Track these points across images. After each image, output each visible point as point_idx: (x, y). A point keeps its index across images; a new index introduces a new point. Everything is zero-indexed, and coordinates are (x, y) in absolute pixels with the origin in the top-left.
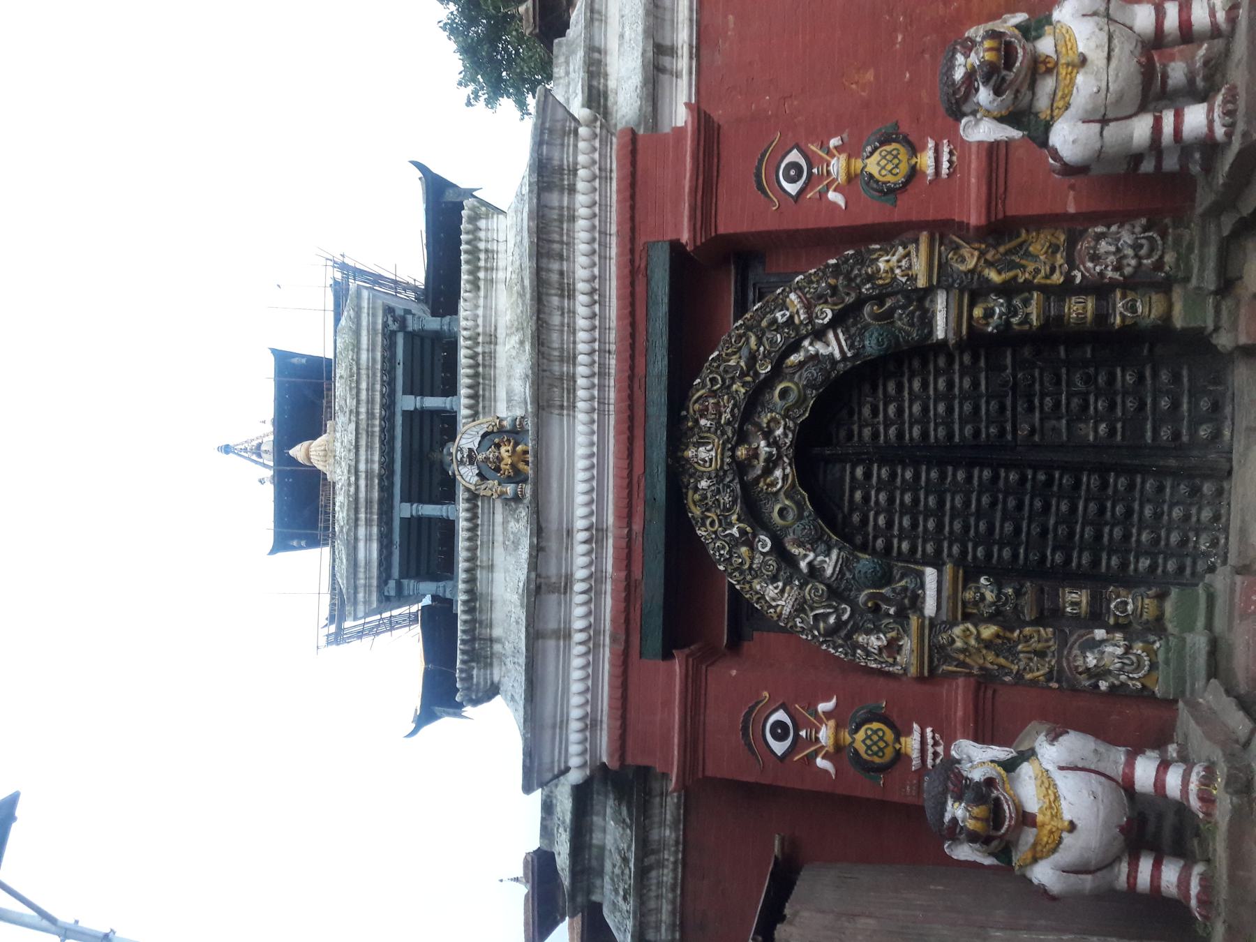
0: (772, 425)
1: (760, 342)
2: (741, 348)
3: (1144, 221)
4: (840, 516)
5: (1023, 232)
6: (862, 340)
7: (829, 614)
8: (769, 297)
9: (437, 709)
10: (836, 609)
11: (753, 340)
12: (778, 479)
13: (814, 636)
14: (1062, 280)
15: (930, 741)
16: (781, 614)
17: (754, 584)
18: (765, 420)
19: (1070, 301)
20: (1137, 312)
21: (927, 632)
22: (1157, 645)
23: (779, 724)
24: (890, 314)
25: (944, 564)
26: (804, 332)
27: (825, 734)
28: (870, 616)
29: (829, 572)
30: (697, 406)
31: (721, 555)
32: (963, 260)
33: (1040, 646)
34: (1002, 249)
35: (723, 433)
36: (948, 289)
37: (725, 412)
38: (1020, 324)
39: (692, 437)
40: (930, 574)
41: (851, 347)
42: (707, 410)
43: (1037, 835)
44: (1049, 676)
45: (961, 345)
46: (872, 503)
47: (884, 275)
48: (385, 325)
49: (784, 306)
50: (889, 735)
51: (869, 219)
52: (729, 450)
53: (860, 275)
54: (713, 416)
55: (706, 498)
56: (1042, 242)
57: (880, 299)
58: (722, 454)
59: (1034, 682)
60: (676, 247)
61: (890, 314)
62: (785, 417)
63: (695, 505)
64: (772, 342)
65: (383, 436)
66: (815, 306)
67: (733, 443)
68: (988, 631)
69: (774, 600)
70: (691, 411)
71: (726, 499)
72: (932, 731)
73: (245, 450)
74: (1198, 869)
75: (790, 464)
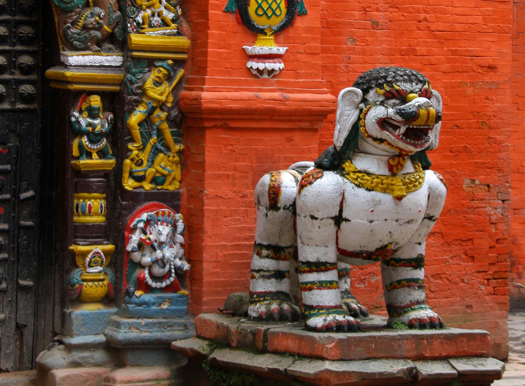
3: (186, 266)
14: (127, 188)
19: (104, 198)
20: (90, 266)
36: (124, 68)
38: (81, 147)
56: (169, 168)
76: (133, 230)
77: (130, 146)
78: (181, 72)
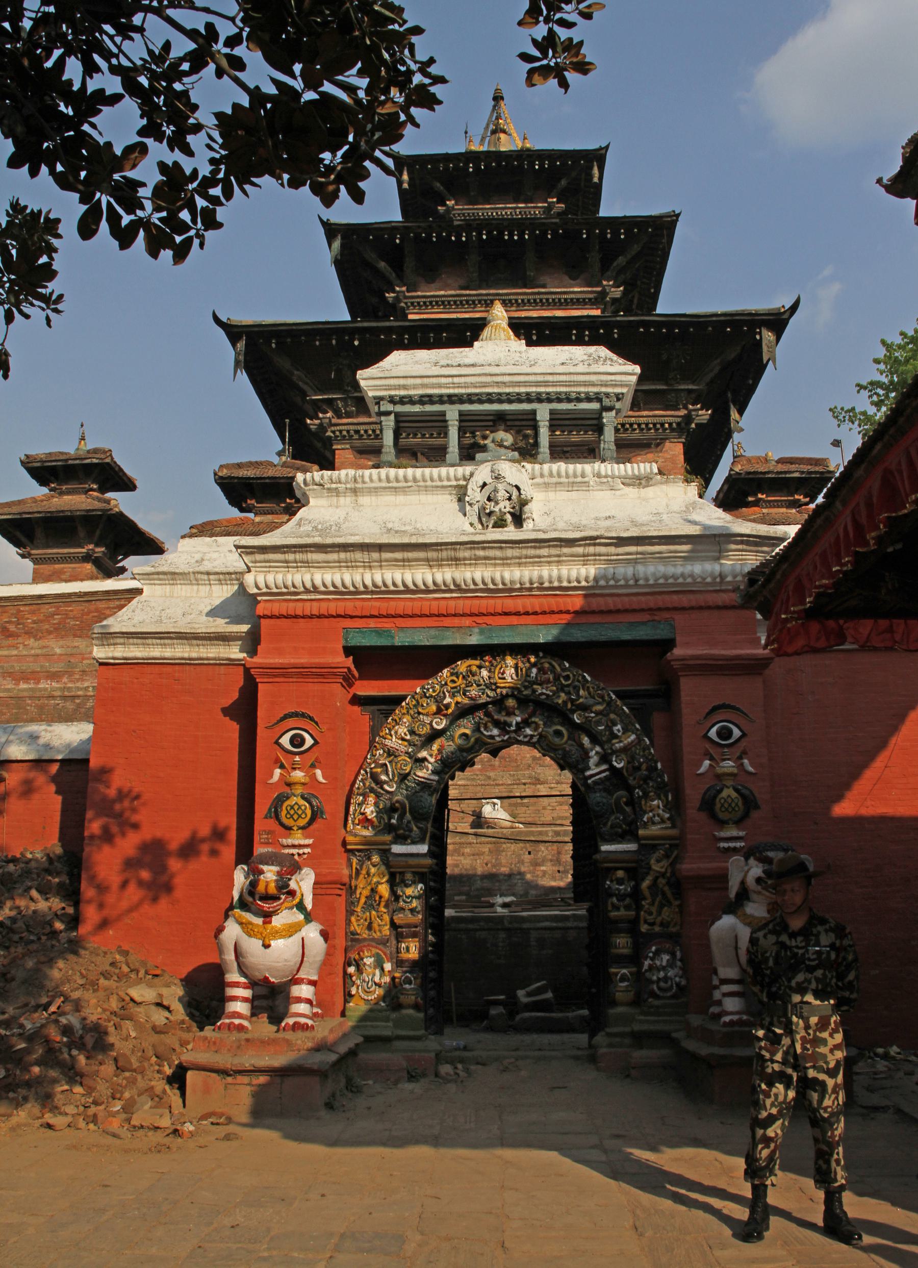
0: (533, 725)
1: (598, 713)
3: (683, 982)
5: (677, 903)
6: (600, 790)
7: (387, 775)
8: (634, 720)
9: (241, 345)
11: (599, 708)
12: (491, 731)
13: (370, 764)
17: (407, 716)
18: (537, 720)
22: (383, 1004)
23: (303, 741)
24: (620, 810)
26: (606, 747)
27: (298, 775)
30: (547, 665)
31: (428, 690)
32: (658, 861)
33: (375, 925)
35: (526, 688)
38: (613, 904)
39: (522, 662)
41: (595, 783)
42: (545, 673)
43: (258, 925)
48: (607, 395)
49: (625, 730)
50: (302, 822)
52: (513, 693)
55: (473, 676)
57: (631, 802)
59: (348, 922)
60: (668, 644)
61: (620, 810)
62: (540, 735)
64: (599, 723)
69: (396, 733)
70: (543, 660)
71: (474, 692)
75: (503, 741)
76: (646, 957)
77: (643, 903)
78: (675, 853)
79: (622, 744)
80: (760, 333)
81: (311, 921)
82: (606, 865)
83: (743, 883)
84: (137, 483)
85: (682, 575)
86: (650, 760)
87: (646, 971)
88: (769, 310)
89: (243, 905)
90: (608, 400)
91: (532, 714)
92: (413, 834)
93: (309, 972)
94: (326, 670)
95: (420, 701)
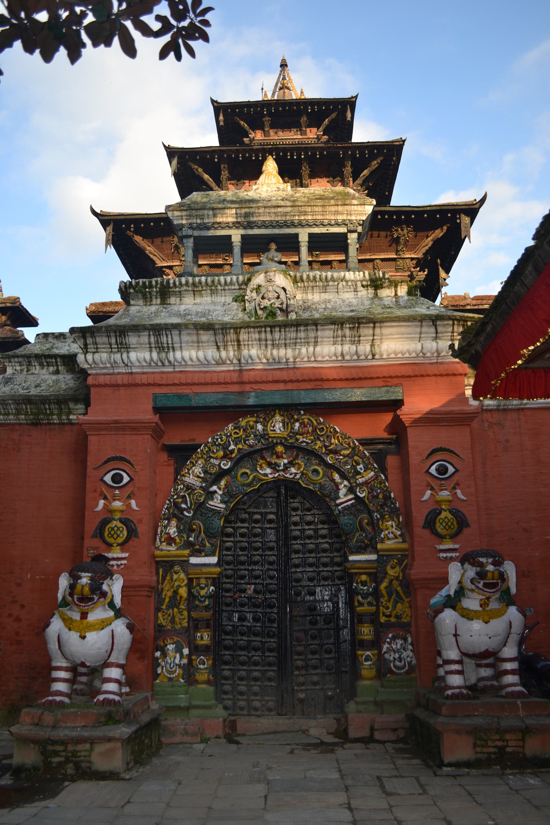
0: (297, 466)
1: (345, 456)
2: (342, 445)
4: (245, 507)
7: (187, 504)
10: (190, 508)
11: (347, 452)
12: (265, 470)
13: (173, 496)
14: (382, 621)
15: (119, 563)
16: (185, 476)
17: (201, 460)
18: (299, 462)
20: (365, 661)
21: (181, 559)
22: (182, 681)
25: (220, 567)
26: (352, 481)
27: (117, 504)
28: (187, 527)
29: (211, 503)
30: (306, 420)
31: (217, 439)
32: (393, 568)
33: (177, 619)
34: (399, 589)
35: (291, 437)
37: (303, 438)
38: (358, 601)
40: (214, 560)
42: (304, 427)
43: (76, 620)
44: (160, 626)
45: (345, 570)
46: (253, 525)
47: (384, 525)
50: (120, 540)
51: (414, 514)
52: (281, 441)
53: (384, 511)
54: (301, 430)
58: (278, 437)
59: (157, 618)
60: (398, 404)
61: (362, 529)
62: (303, 473)
63: (247, 422)
64: (346, 463)
65: (282, 222)
66: (367, 487)
67: (285, 443)
68: (183, 592)
69: (193, 472)
72: (125, 564)
73: (284, 79)
74: (66, 700)
75: (274, 477)
76: (384, 644)
79: (363, 479)
80: (460, 218)
81: (120, 617)
82: (353, 571)
83: (460, 582)
84: (39, 322)
85: (408, 351)
86: (385, 491)
87: (385, 653)
88: (465, 202)
89: (65, 603)
90: (352, 225)
91: (296, 457)
92: (206, 549)
93: (118, 657)
94: (139, 425)
95: (211, 448)
